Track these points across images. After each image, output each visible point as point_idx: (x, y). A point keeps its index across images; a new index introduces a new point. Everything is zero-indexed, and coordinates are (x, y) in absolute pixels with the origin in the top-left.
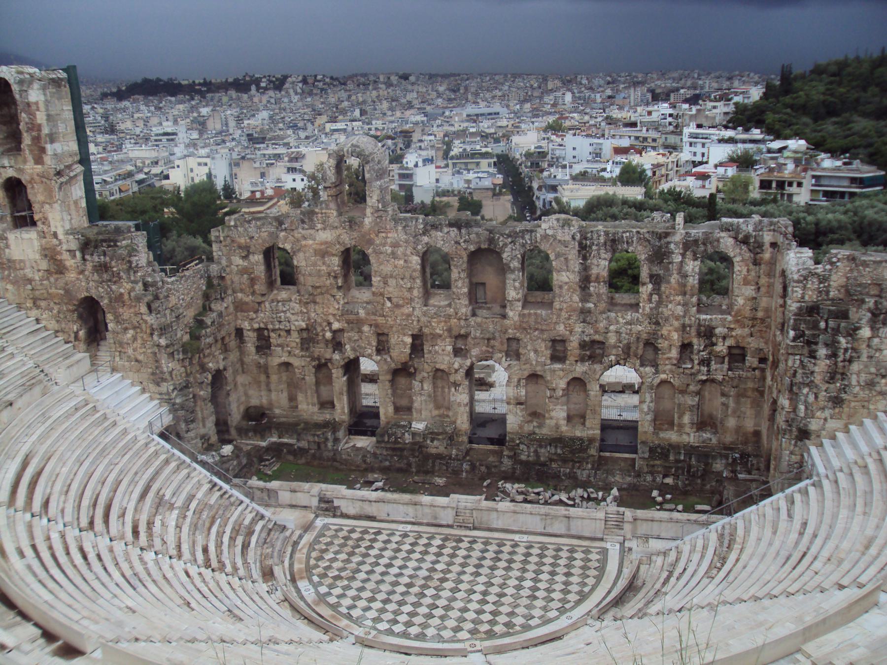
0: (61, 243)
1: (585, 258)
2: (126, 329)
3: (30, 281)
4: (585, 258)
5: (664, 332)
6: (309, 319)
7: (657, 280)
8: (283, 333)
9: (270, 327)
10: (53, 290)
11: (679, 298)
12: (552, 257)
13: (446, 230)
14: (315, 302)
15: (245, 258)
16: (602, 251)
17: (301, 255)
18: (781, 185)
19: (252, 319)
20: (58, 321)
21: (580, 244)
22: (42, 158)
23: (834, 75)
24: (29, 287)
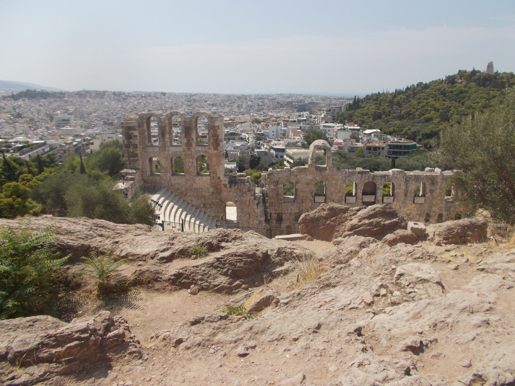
0: (221, 181)
1: (407, 184)
2: (246, 215)
3: (204, 197)
4: (407, 184)
5: (434, 210)
6: (300, 208)
7: (432, 191)
8: (288, 215)
9: (283, 212)
10: (214, 200)
11: (439, 198)
12: (395, 184)
13: (356, 175)
14: (303, 202)
15: (275, 186)
16: (413, 182)
17: (299, 184)
18: (375, 148)
19: (277, 210)
20: (215, 213)
21: (406, 179)
22: (217, 148)
23: (374, 100)
24: (203, 199)
